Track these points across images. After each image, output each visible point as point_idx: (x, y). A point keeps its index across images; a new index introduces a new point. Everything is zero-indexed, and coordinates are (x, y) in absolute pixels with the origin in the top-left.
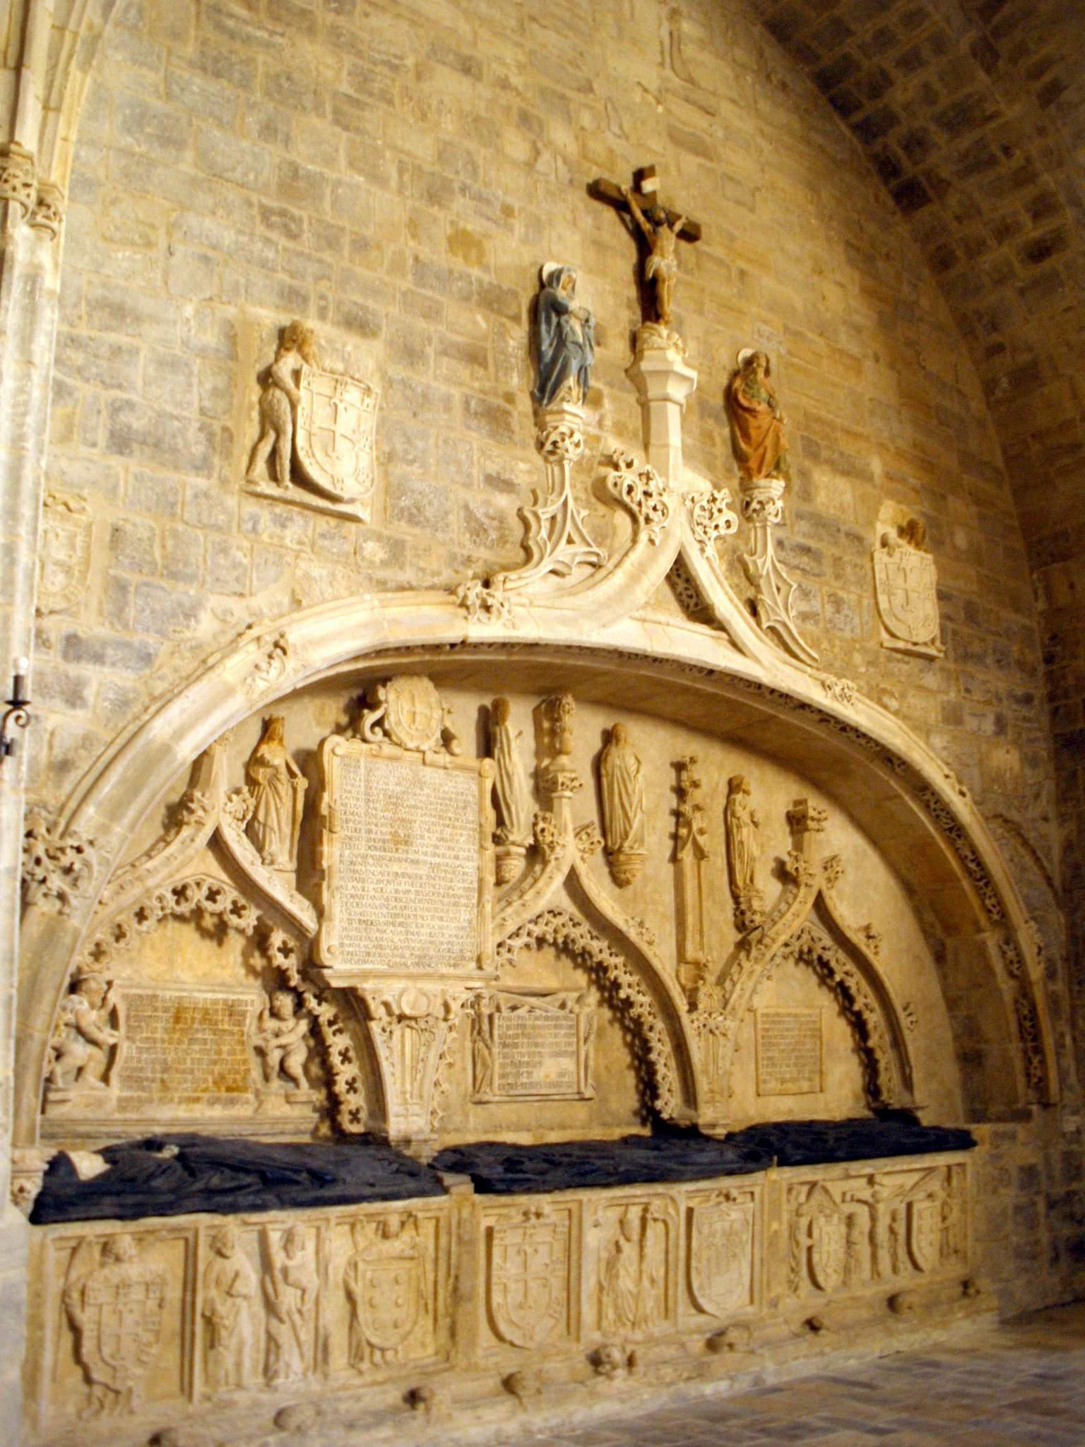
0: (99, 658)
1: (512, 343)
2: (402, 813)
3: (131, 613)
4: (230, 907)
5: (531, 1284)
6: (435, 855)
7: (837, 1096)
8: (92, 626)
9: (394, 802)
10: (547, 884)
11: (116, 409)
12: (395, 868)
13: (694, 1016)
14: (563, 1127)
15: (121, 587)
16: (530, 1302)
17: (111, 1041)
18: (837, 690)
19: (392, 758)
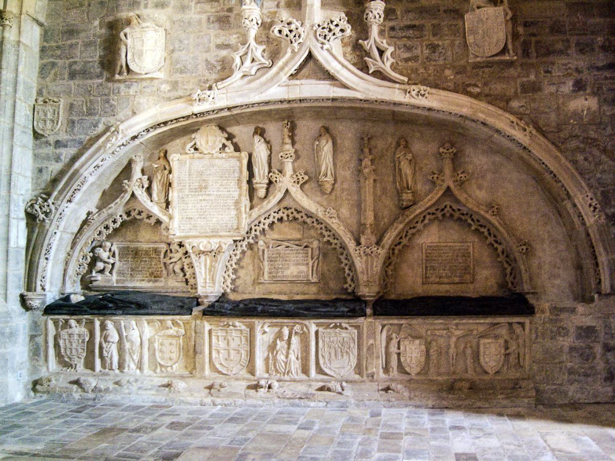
0: (66, 146)
2: (204, 177)
3: (76, 129)
5: (232, 352)
8: (63, 137)
9: (201, 174)
10: (274, 197)
12: (201, 198)
15: (73, 122)
17: (112, 262)
18: (414, 93)
19: (199, 158)
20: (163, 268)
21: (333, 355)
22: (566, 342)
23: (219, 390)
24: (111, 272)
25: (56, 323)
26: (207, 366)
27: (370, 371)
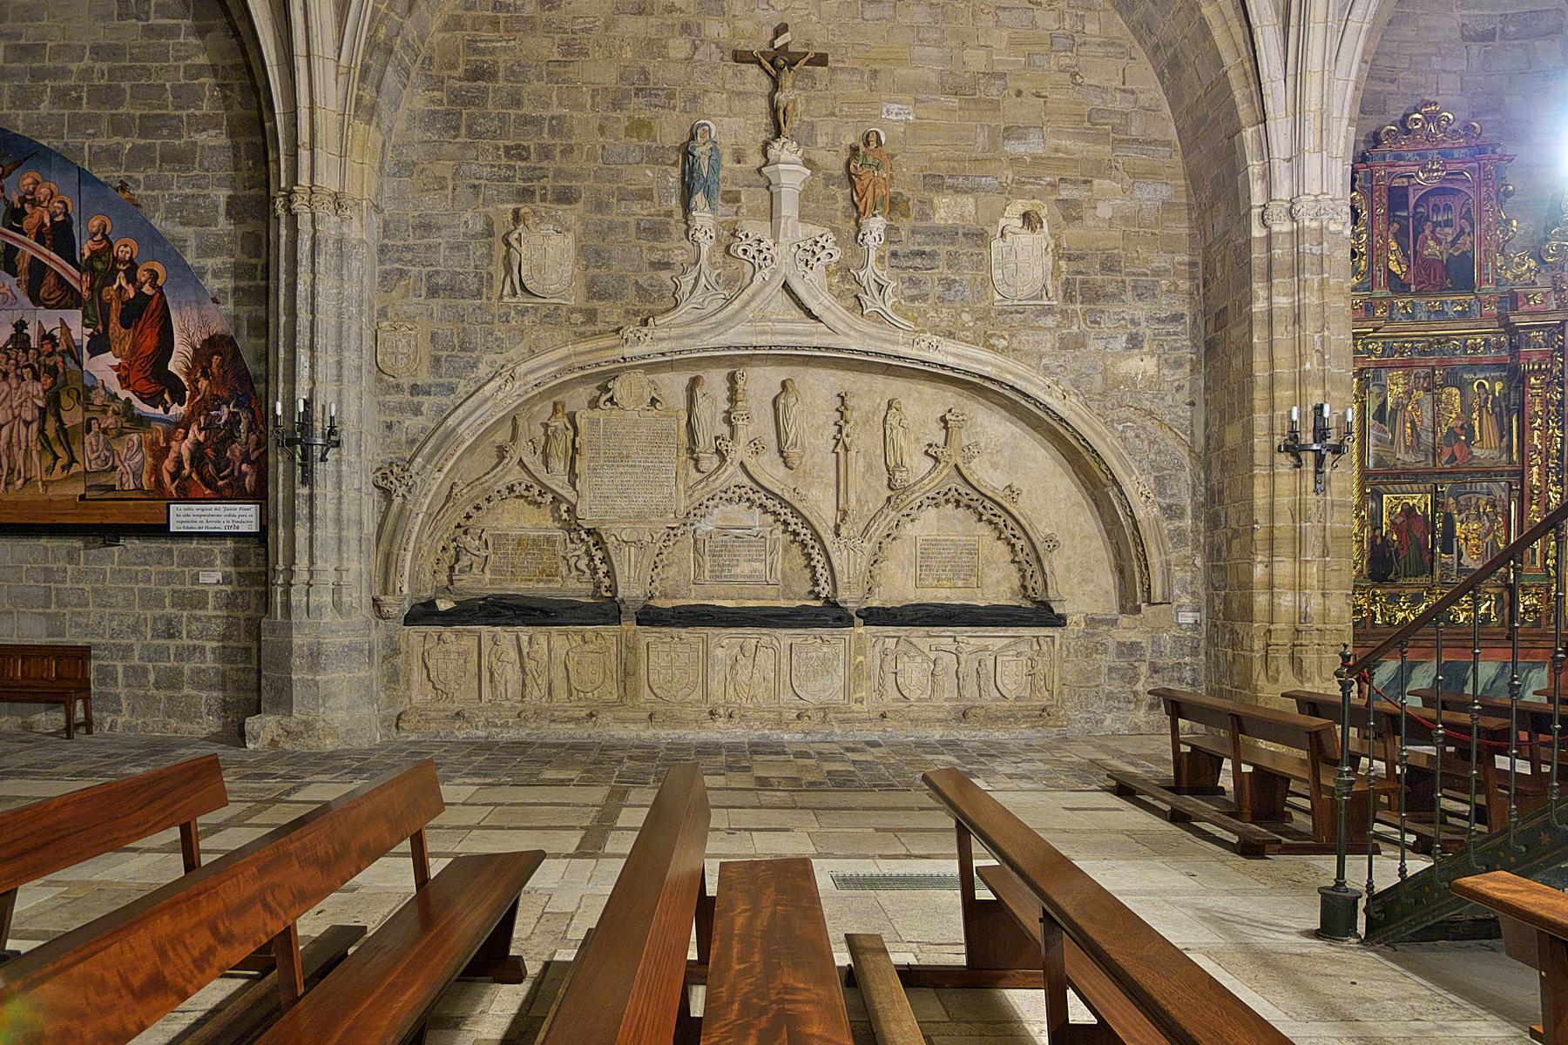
0: (429, 393)
8: (424, 378)
11: (429, 276)
15: (437, 360)
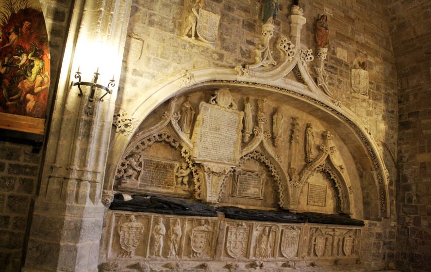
0: (141, 75)
1: (257, 7)
4: (172, 140)
5: (237, 242)
6: (226, 134)
7: (329, 208)
12: (216, 135)
13: (291, 182)
14: (254, 205)
16: (237, 247)
17: (139, 170)
18: (337, 103)
20: (175, 180)
21: (287, 245)
22: (373, 240)
23: (235, 269)
24: (137, 178)
25: (118, 217)
26: (223, 252)
27: (303, 255)
